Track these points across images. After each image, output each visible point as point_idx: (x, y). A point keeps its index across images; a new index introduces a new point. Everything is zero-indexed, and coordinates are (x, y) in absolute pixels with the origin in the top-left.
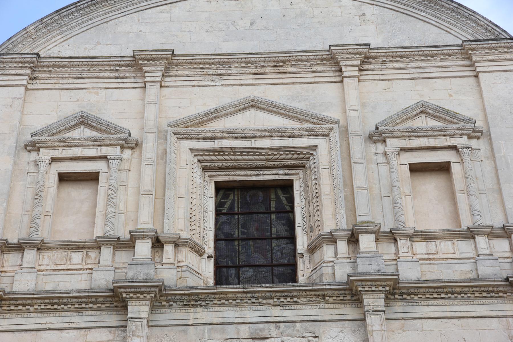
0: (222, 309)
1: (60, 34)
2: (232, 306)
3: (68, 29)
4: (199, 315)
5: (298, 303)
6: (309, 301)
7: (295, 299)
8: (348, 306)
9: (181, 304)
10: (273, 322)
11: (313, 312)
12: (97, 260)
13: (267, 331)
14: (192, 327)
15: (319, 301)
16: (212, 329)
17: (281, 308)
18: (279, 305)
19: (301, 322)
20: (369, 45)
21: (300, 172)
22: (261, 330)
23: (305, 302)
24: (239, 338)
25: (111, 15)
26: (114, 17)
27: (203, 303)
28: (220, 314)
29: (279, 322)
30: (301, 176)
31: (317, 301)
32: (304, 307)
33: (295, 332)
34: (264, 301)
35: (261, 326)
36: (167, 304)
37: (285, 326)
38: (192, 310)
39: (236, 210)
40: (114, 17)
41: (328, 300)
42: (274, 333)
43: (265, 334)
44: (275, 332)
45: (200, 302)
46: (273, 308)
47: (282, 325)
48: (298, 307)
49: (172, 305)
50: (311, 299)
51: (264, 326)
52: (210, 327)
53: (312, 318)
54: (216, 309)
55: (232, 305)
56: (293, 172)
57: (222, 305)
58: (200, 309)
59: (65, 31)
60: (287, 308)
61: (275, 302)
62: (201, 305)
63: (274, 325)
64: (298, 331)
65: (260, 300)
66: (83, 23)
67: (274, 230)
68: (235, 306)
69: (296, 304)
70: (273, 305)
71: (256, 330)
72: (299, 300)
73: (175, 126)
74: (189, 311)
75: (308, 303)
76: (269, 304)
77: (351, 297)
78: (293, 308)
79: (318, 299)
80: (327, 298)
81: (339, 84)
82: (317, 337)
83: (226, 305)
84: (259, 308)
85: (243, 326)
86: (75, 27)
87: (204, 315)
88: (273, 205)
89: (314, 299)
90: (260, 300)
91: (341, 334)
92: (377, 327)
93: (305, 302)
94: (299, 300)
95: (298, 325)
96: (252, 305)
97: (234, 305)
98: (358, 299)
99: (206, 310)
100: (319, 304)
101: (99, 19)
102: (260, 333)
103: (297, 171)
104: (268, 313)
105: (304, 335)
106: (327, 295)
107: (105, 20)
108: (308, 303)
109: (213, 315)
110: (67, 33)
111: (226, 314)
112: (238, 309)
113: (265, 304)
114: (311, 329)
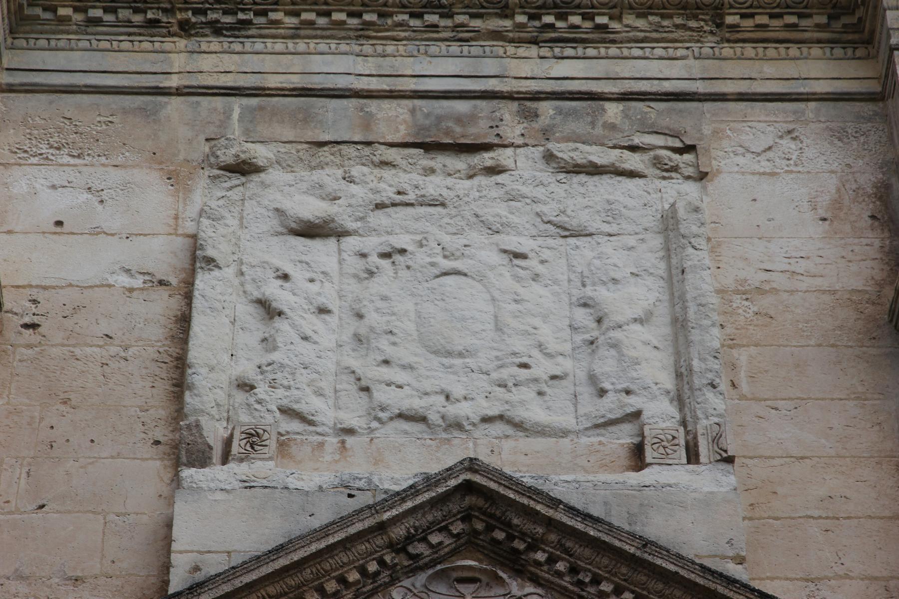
0: (301, 46)
2: (344, 38)
4: (206, 63)
5: (612, 36)
6: (658, 28)
7: (601, 20)
8: (816, 51)
9: (138, 18)
10: (509, 97)
11: (675, 69)
13: (483, 124)
14: (176, 102)
15: (699, 30)
16: (261, 108)
17: (545, 52)
18: (535, 42)
19: (624, 97)
22: (459, 120)
23: (642, 35)
24: (369, 144)
27: (228, 19)
28: (297, 63)
29: (536, 97)
31: (691, 29)
32: (637, 52)
33: (599, 131)
34: (476, 23)
35: (462, 106)
36: (79, 17)
37: (559, 111)
38: (182, 43)
41: (734, 27)
42: (513, 130)
43: (478, 132)
44: (519, 129)
45: (212, 16)
46: (511, 50)
47: (547, 108)
48: (613, 51)
49: (97, 22)
50: (665, 23)
51: (475, 107)
52: (254, 101)
53: (668, 86)
54: (279, 46)
55: (343, 34)
57: (302, 32)
58: (214, 43)
60: (569, 52)
61: (520, 27)
62: (217, 30)
63: (514, 106)
64: (613, 127)
65: (460, 19)
68: (358, 38)
69: (603, 41)
70: (512, 41)
71: (440, 119)
72: (615, 25)
74: (168, 46)
75: (655, 35)
76: (496, 35)
77: (830, 17)
78: (591, 52)
79: (693, 24)
80: (730, 20)
82: (690, 149)
83: (319, 32)
84: (455, 48)
85: (386, 104)
87: (229, 62)
89: (678, 21)
90: (460, 19)
91: (786, 142)
93: (642, 35)
94: (615, 25)
95: (613, 110)
96: (426, 36)
97: (351, 34)
98: (857, 27)
99: (237, 47)
100: (698, 41)
102: (458, 129)
104: (489, 66)
105: (637, 140)
106: (731, 7)
108: (655, 35)
109: (269, 63)
111: (317, 63)
112: (367, 49)
113: (478, 35)
114: (666, 122)
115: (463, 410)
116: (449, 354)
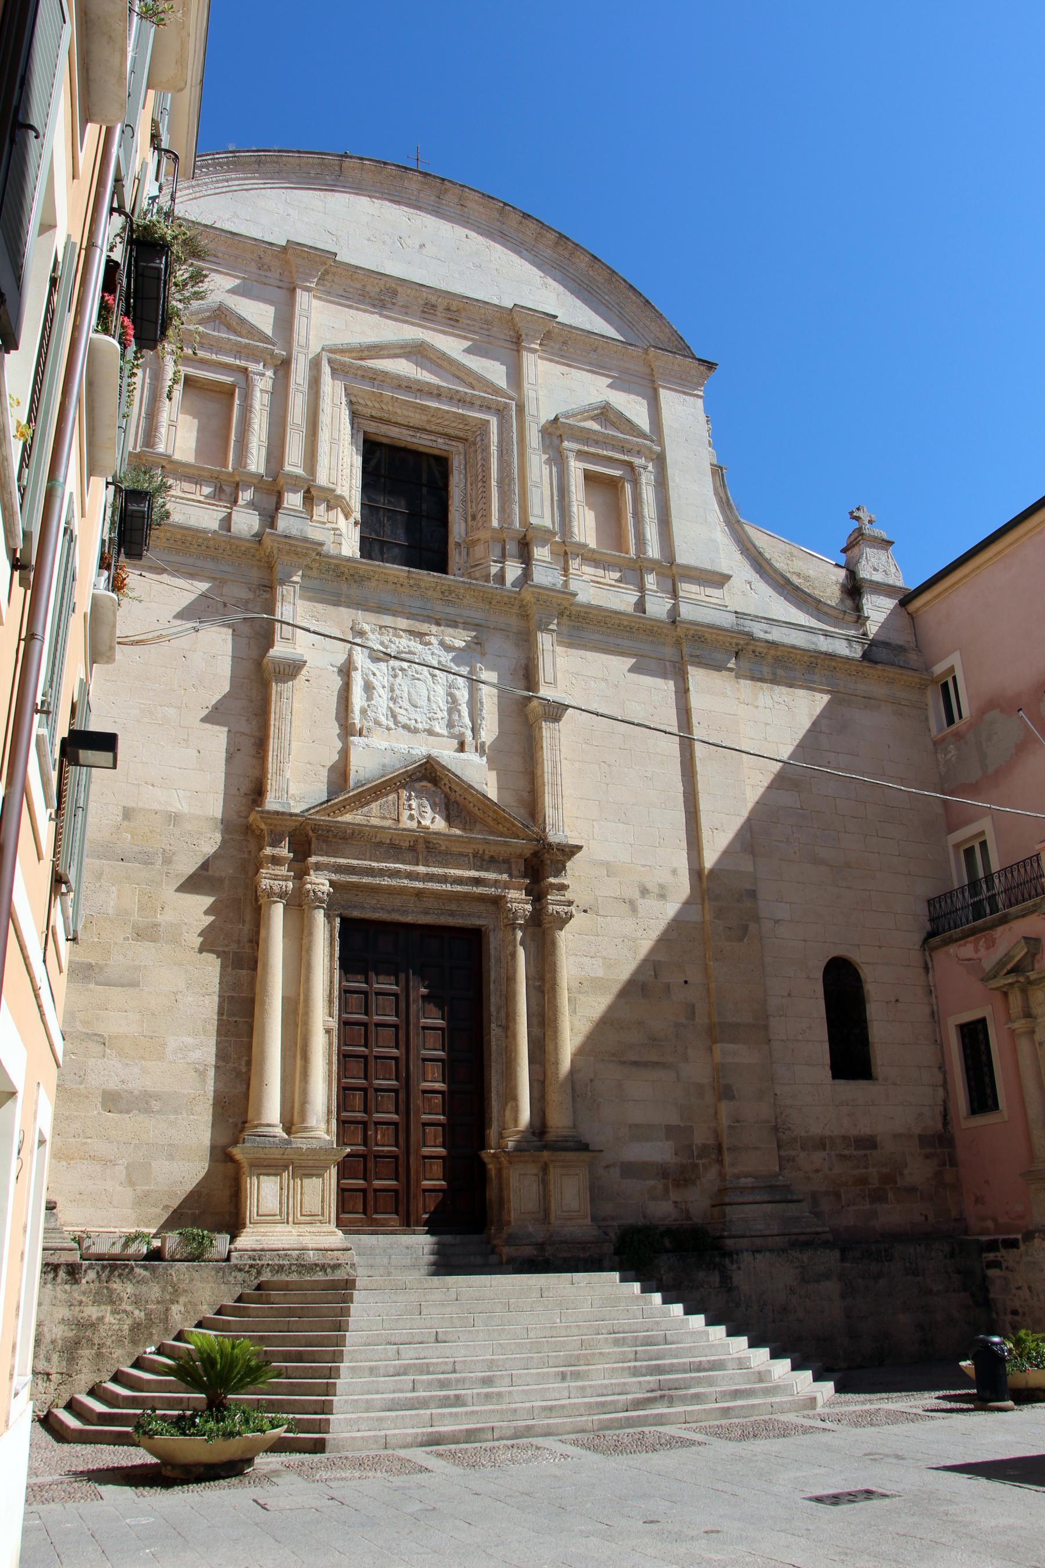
1: (188, 188)
3: (198, 185)
12: (233, 497)
20: (556, 317)
21: (461, 446)
25: (252, 181)
26: (256, 186)
30: (462, 450)
39: (383, 472)
40: (256, 186)
56: (453, 443)
59: (193, 187)
66: (217, 182)
67: (424, 507)
73: (331, 351)
81: (515, 353)
86: (206, 184)
88: (425, 476)
92: (548, 646)
101: (237, 182)
103: (458, 444)
107: (245, 187)
110: (197, 189)
115: (420, 726)
116: (416, 707)
